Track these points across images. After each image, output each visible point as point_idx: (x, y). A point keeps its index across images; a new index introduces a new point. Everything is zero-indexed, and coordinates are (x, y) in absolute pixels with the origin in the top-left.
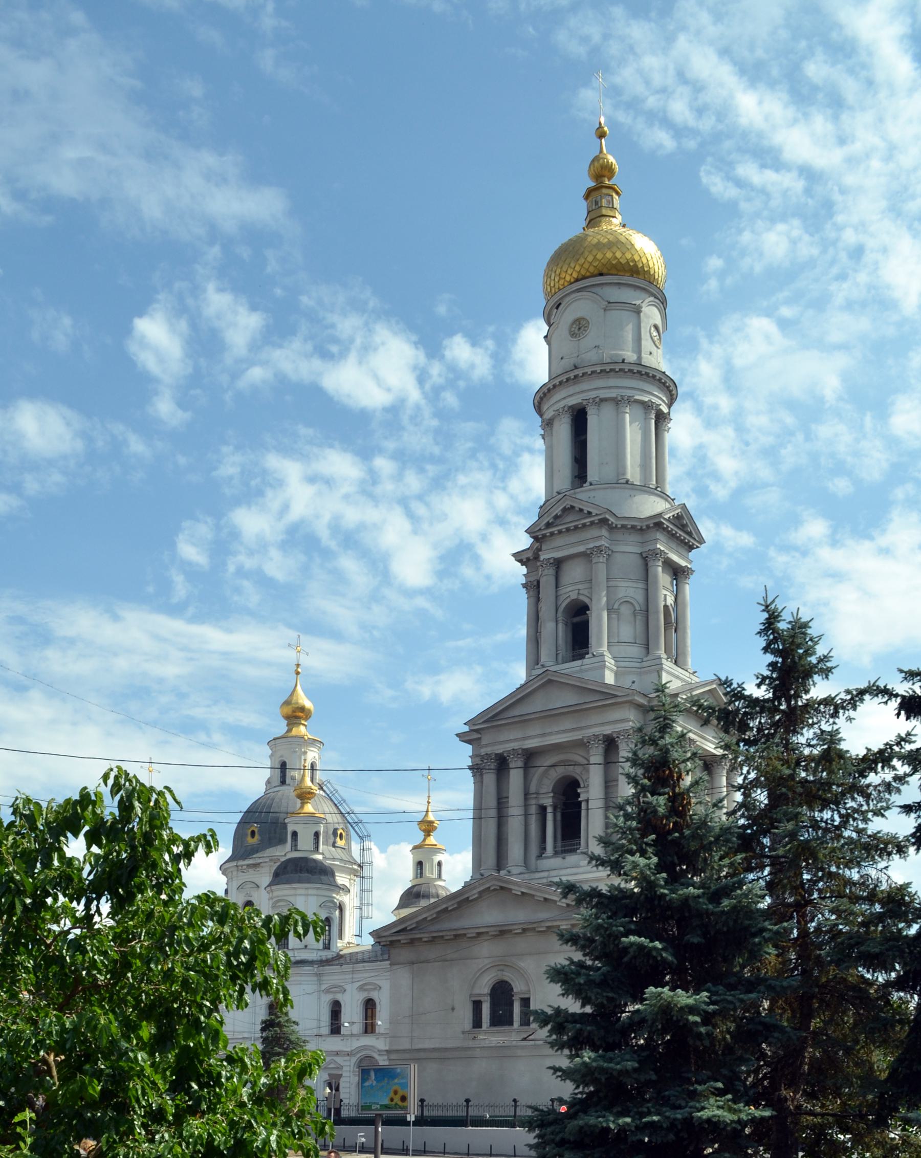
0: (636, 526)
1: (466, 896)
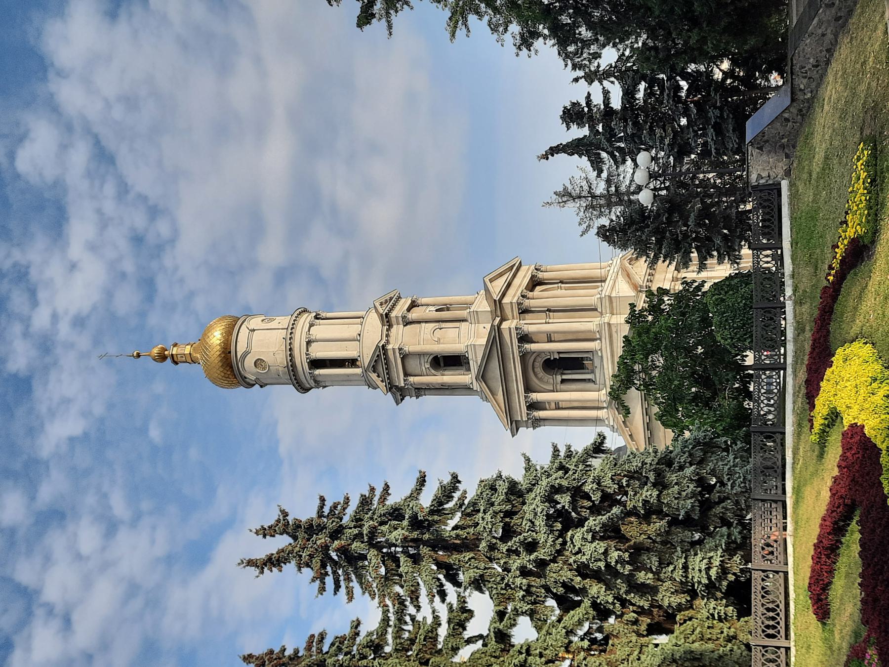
1: (622, 423)
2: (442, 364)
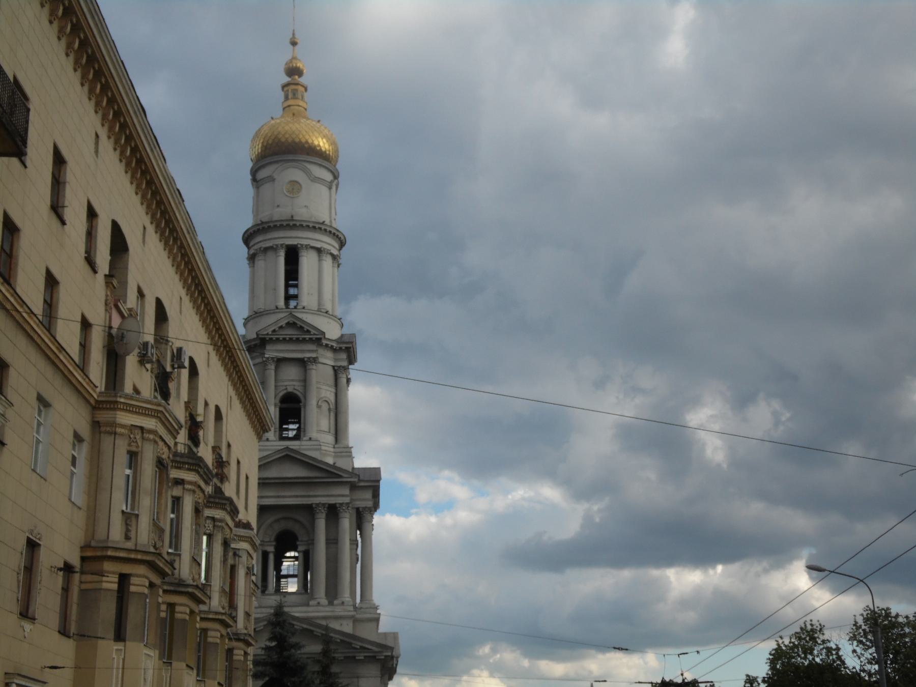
0: (333, 346)
2: (285, 406)
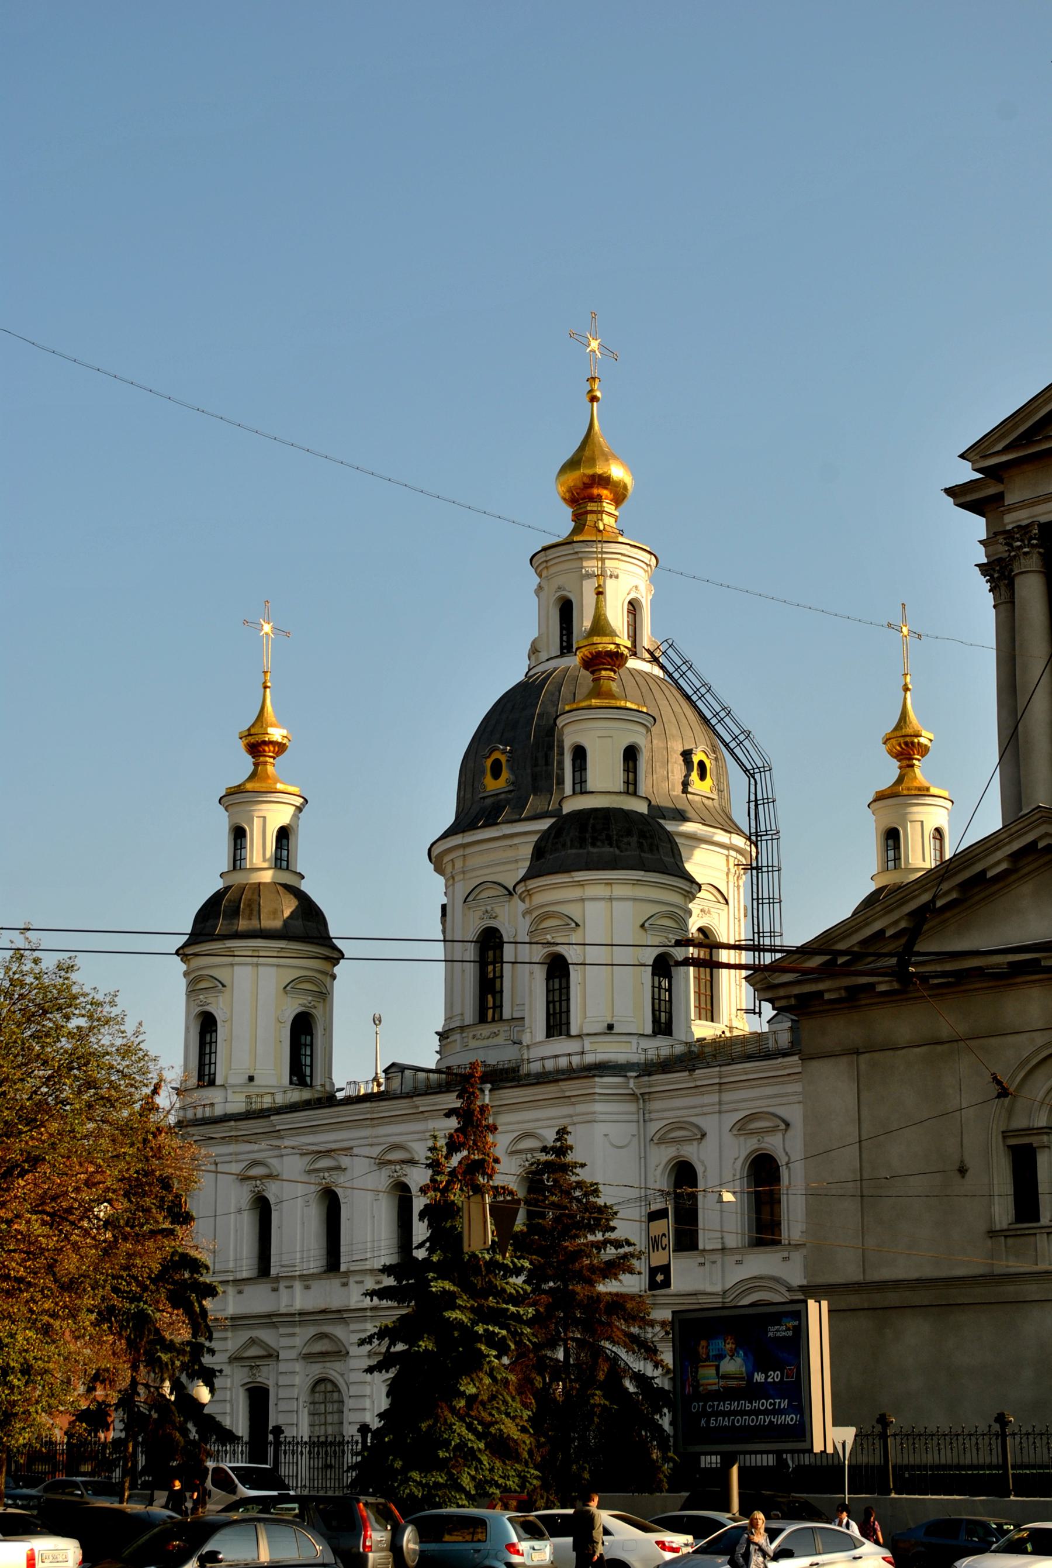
1: (978, 868)
